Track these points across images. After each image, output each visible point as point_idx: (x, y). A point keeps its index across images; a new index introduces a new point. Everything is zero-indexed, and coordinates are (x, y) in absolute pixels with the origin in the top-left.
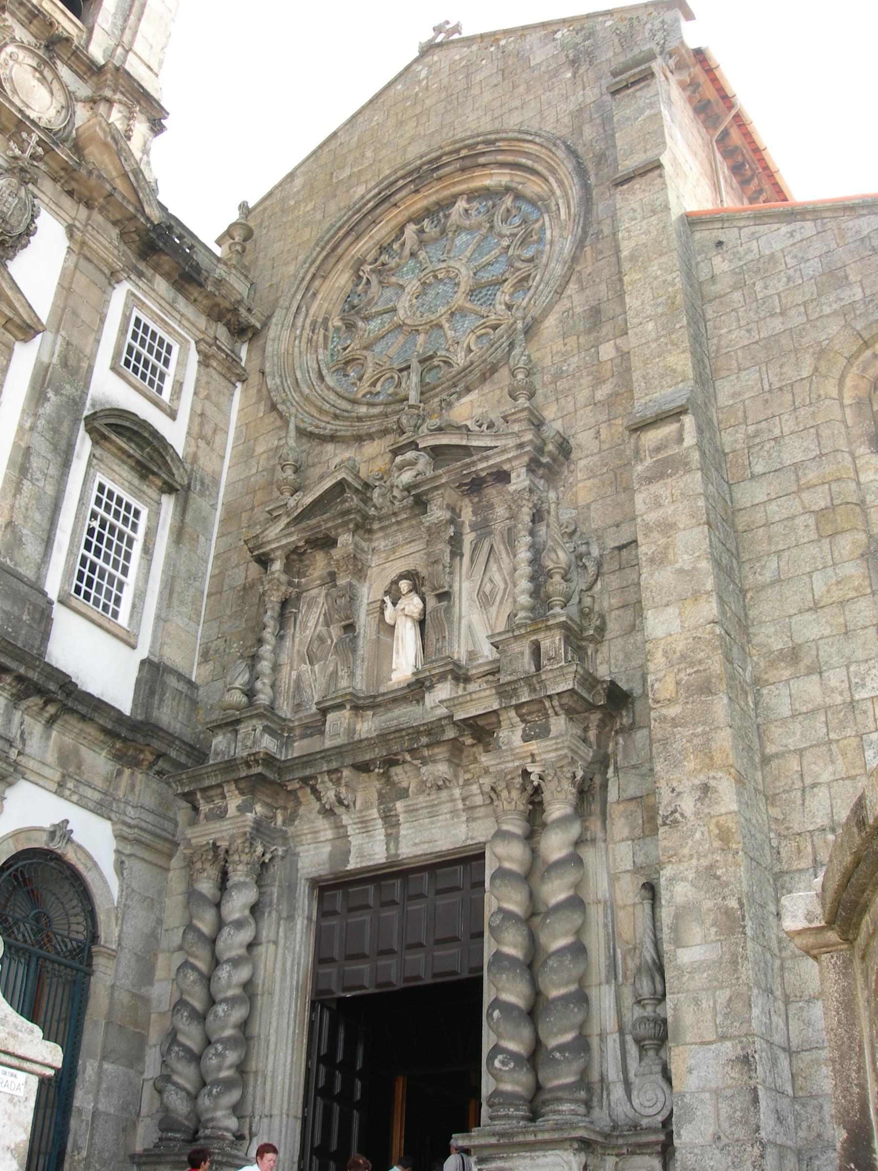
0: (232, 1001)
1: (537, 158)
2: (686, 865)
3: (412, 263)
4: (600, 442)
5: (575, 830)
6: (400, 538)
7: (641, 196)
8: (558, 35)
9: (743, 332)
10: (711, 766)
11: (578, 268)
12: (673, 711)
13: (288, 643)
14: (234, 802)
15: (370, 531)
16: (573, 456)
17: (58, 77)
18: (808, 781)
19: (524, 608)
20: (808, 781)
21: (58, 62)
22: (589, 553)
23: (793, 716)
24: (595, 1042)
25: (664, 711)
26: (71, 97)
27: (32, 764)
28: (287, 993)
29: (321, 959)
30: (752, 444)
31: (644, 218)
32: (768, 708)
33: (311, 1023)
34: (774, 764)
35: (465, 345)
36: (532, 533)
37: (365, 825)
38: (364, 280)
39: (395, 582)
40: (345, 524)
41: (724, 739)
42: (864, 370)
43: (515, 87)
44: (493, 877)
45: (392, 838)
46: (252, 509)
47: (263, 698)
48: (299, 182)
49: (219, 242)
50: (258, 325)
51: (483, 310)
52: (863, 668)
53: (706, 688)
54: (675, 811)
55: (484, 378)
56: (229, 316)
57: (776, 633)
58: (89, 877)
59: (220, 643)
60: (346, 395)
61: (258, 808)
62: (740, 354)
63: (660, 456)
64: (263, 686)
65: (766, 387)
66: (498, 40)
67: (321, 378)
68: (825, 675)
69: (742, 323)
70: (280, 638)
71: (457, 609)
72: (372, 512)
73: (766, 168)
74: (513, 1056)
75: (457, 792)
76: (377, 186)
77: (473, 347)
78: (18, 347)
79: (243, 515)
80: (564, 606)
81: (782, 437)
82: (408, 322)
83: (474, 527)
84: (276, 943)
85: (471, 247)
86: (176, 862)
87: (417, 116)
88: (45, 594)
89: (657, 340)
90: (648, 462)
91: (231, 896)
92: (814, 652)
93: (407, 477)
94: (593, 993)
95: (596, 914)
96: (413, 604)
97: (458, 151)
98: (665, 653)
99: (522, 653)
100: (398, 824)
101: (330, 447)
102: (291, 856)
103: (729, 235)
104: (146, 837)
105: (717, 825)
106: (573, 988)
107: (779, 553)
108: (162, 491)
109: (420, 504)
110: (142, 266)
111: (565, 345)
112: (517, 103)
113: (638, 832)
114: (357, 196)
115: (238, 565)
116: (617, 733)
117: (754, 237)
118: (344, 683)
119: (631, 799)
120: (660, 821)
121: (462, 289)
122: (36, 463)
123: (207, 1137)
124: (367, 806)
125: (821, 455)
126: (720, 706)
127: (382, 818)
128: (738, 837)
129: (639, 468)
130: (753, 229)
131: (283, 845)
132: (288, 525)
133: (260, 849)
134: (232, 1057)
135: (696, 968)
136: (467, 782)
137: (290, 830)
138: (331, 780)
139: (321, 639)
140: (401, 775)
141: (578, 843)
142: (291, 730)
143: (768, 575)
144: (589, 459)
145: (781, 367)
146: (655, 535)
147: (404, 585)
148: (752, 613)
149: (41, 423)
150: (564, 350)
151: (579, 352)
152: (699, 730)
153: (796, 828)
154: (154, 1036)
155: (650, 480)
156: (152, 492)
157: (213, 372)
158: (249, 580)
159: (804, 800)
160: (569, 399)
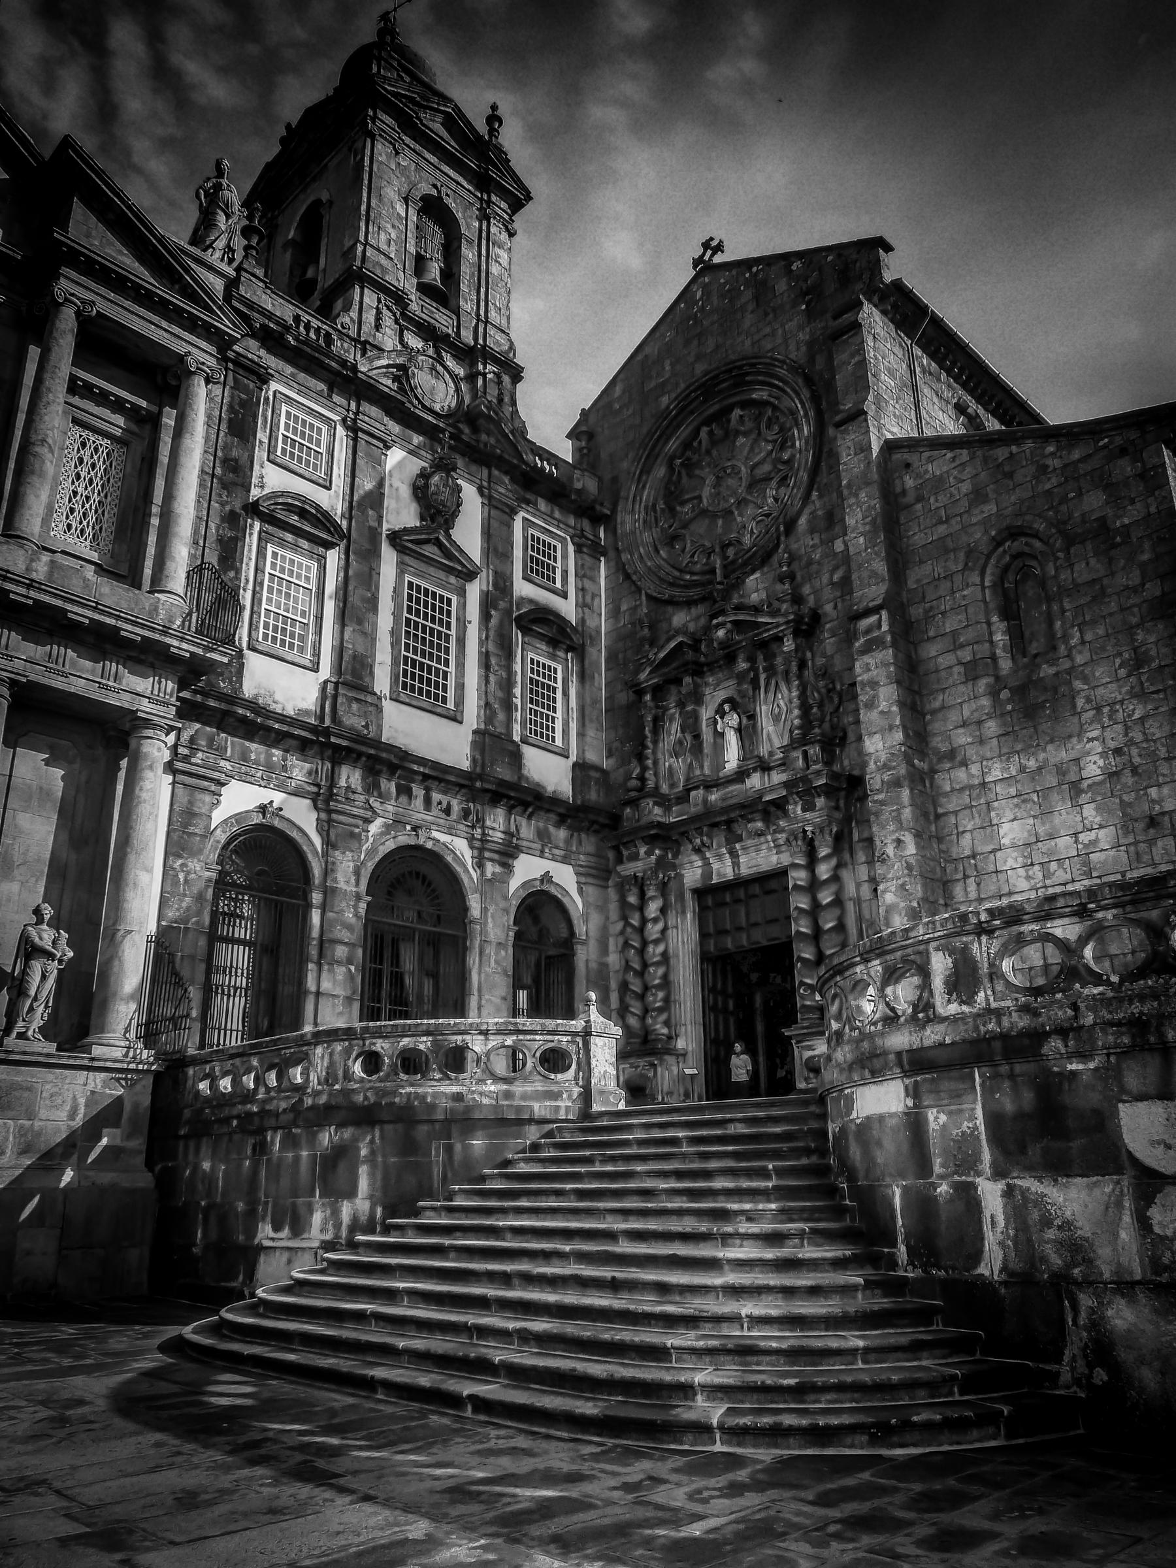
0: (657, 964)
1: (785, 382)
3: (707, 459)
5: (834, 862)
6: (720, 675)
8: (794, 267)
11: (818, 479)
12: (881, 797)
13: (661, 745)
16: (823, 620)
17: (446, 368)
18: (961, 829)
20: (961, 829)
21: (444, 354)
22: (834, 688)
23: (953, 790)
27: (525, 843)
29: (704, 935)
30: (929, 617)
31: (856, 454)
32: (938, 787)
34: (943, 819)
36: (800, 676)
37: (720, 857)
39: (721, 705)
40: (686, 671)
41: (907, 813)
42: (998, 562)
43: (766, 314)
45: (736, 864)
47: (651, 784)
48: (618, 390)
52: (990, 763)
53: (896, 783)
57: (942, 741)
58: (565, 900)
61: (657, 852)
64: (649, 774)
72: (702, 659)
75: (769, 838)
76: (676, 398)
78: (468, 587)
79: (620, 656)
80: (820, 727)
84: (677, 927)
85: (747, 449)
86: (610, 883)
88: (514, 742)
89: (866, 549)
90: (862, 640)
93: (721, 633)
95: (850, 907)
96: (733, 719)
97: (730, 371)
98: (875, 763)
100: (738, 856)
101: (670, 609)
102: (680, 877)
103: (913, 458)
104: (593, 872)
108: (567, 652)
109: (731, 659)
110: (529, 496)
112: (768, 330)
114: (663, 406)
117: (930, 460)
118: (698, 772)
121: (743, 484)
122: (493, 661)
123: (655, 1040)
124: (719, 847)
125: (967, 626)
126: (905, 794)
128: (916, 868)
132: (650, 673)
133: (661, 876)
134: (661, 995)
136: (775, 832)
137: (677, 862)
139: (680, 742)
140: (738, 829)
141: (839, 866)
142: (669, 800)
143: (937, 704)
146: (868, 689)
147: (727, 707)
148: (929, 728)
149: (492, 633)
150: (811, 543)
153: (955, 857)
154: (614, 985)
156: (561, 654)
157: (586, 557)
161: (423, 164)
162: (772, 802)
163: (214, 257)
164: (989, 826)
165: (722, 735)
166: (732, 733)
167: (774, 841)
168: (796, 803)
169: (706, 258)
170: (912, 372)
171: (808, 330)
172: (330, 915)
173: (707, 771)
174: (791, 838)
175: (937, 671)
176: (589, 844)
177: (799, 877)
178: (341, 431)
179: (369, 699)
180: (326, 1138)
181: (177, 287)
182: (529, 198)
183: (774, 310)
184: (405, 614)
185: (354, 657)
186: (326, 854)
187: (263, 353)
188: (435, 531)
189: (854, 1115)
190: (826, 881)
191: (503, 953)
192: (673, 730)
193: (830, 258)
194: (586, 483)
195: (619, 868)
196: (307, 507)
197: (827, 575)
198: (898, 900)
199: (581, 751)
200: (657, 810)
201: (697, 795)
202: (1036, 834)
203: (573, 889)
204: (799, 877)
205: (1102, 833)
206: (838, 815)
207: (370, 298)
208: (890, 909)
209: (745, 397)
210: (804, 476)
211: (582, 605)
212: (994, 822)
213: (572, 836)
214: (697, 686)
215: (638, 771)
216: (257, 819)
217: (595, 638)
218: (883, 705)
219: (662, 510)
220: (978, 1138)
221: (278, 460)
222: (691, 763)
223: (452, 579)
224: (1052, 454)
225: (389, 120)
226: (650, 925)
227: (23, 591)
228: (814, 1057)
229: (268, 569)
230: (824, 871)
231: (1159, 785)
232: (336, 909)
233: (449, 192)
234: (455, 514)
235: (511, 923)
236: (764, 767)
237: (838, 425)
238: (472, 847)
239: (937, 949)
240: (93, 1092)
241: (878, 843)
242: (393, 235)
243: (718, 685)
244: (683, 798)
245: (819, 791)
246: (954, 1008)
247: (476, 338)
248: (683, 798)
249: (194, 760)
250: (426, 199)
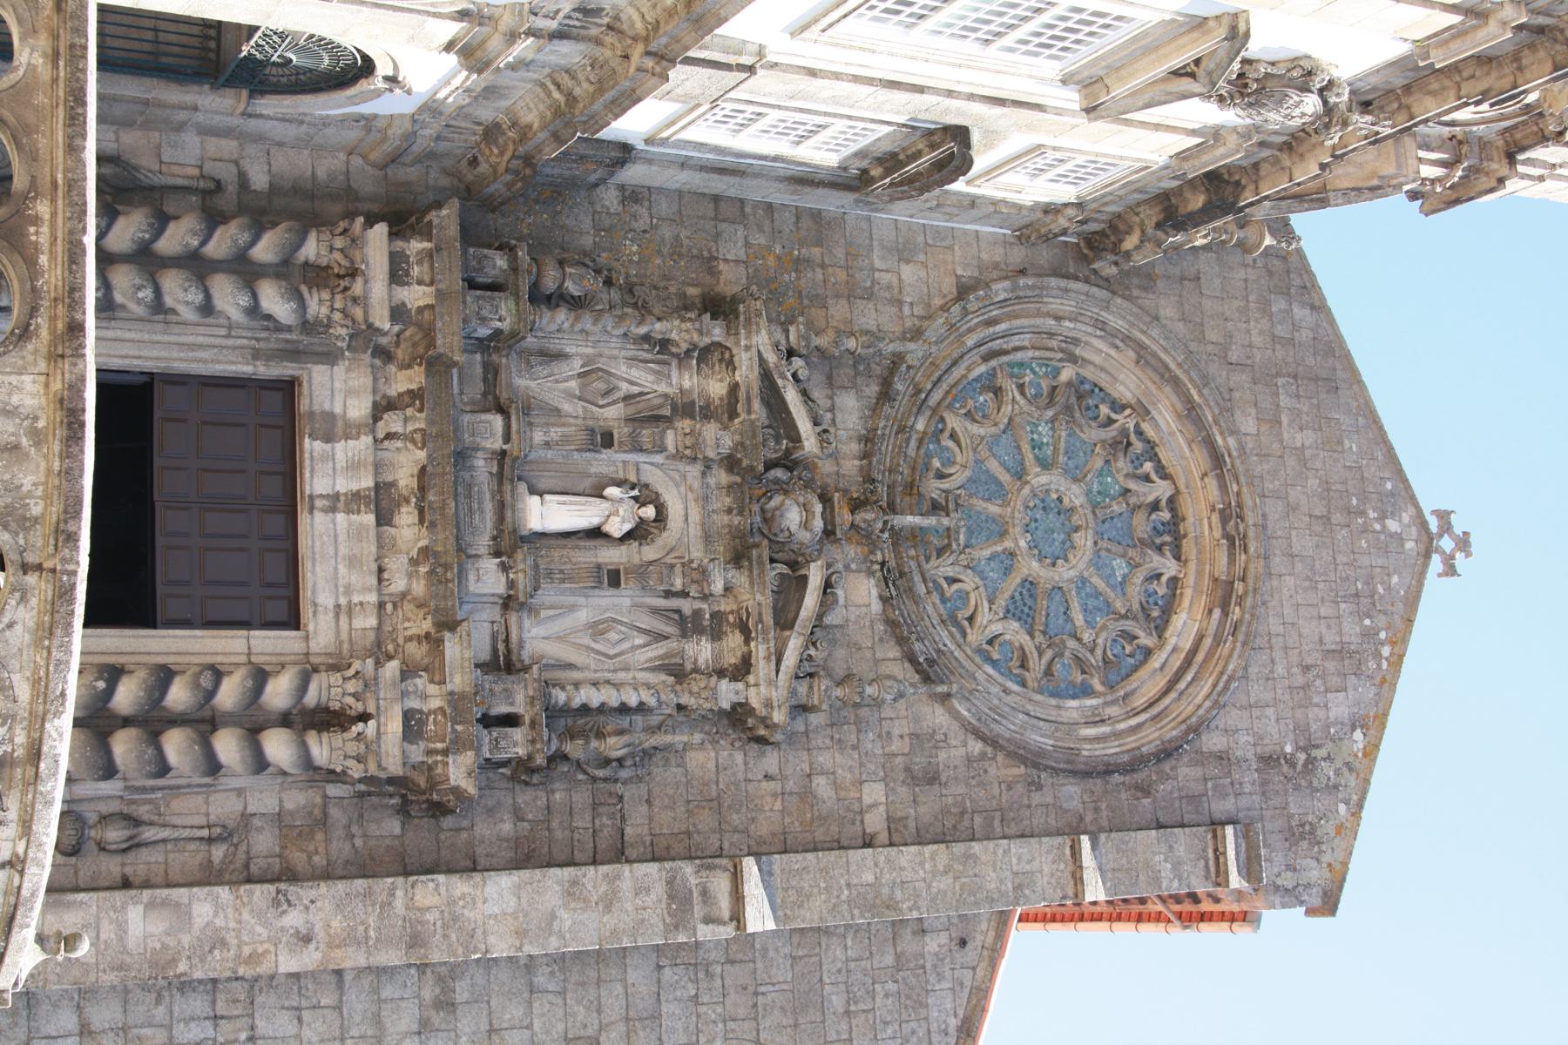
2: (231, 916)
4: (759, 781)
7: (1046, 870)
8: (1358, 735)
9: (839, 965)
10: (330, 946)
11: (1000, 757)
19: (569, 699)
20: (306, 1015)
23: (380, 1001)
25: (399, 893)
28: (164, 354)
35: (962, 577)
37: (353, 467)
38: (1114, 416)
45: (334, 502)
46: (823, 266)
50: (1095, 266)
53: (416, 940)
54: (288, 901)
55: (891, 624)
56: (1113, 239)
59: (643, 223)
62: (814, 959)
63: (695, 895)
65: (762, 989)
66: (1393, 644)
68: (416, 1039)
69: (852, 965)
73: (1119, 918)
77: (956, 586)
79: (816, 251)
81: (697, 1003)
82: (1026, 490)
83: (697, 614)
84: (228, 336)
87: (1326, 519)
90: (693, 881)
91: (289, 300)
92: (443, 1026)
97: (1243, 579)
98: (463, 897)
99: (512, 704)
100: (349, 511)
101: (873, 389)
105: (267, 952)
107: (562, 993)
111: (902, 737)
112: (1280, 670)
113: (287, 820)
115: (747, 244)
116: (403, 796)
119: (325, 814)
120: (283, 886)
127: (359, 491)
130: (968, 984)
131: (349, 346)
132: (762, 361)
135: (122, 929)
138: (415, 431)
144: (743, 767)
145: (782, 1008)
146: (604, 888)
147: (649, 512)
150: (896, 732)
151: (885, 755)
152: (372, 934)
153: (260, 1000)
155: (670, 882)
158: (722, 266)
159: (287, 1009)
160: (828, 741)
166: (595, 521)
167: (361, 604)
171: (1250, 755)
183: (1306, 687)
193: (1342, 808)
197: (829, 764)
198: (196, 931)
208: (183, 913)
213: (479, 124)
218: (566, 918)
236: (508, 603)
241: (313, 893)
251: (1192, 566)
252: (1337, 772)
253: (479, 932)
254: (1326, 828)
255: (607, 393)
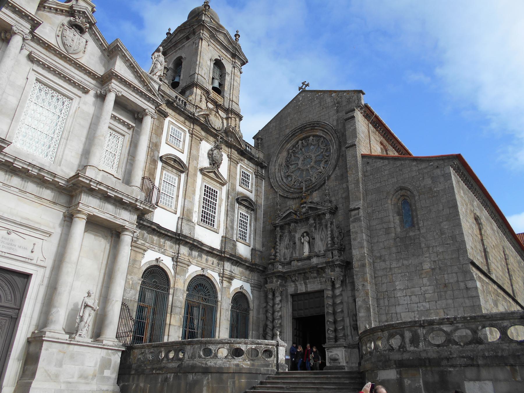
0: (278, 319)
5: (341, 289)
8: (333, 95)
13: (282, 245)
14: (275, 280)
15: (298, 222)
16: (338, 209)
17: (219, 115)
19: (329, 244)
20: (383, 282)
21: (219, 110)
24: (346, 328)
25: (356, 270)
26: (222, 119)
29: (293, 310)
33: (293, 322)
36: (330, 227)
37: (301, 284)
39: (303, 233)
43: (323, 109)
44: (326, 298)
45: (306, 287)
49: (253, 138)
51: (318, 167)
55: (319, 188)
58: (247, 295)
60: (289, 185)
61: (280, 281)
67: (283, 180)
70: (280, 243)
71: (316, 242)
74: (332, 331)
75: (318, 279)
82: (301, 168)
83: (319, 224)
85: (314, 150)
87: (300, 112)
88: (234, 241)
90: (353, 218)
93: (304, 210)
94: (345, 319)
95: (345, 304)
96: (307, 238)
97: (310, 124)
101: (286, 199)
102: (287, 290)
103: (370, 161)
106: (341, 318)
108: (251, 211)
110: (242, 158)
112: (323, 114)
114: (287, 133)
117: (375, 162)
119: (351, 283)
122: (229, 212)
129: (351, 219)
136: (320, 277)
139: (289, 245)
142: (284, 264)
143: (376, 241)
147: (305, 234)
149: (229, 204)
156: (250, 212)
161: (216, 48)
162: (321, 268)
163: (156, 78)
164: (392, 282)
165: (303, 243)
168: (328, 269)
169: (303, 87)
170: (369, 132)
172: (175, 297)
173: (297, 255)
174: (327, 280)
175: (376, 230)
176: (255, 276)
177: (329, 293)
178: (188, 135)
179: (192, 224)
180: (191, 377)
181: (145, 87)
182: (247, 62)
184: (203, 196)
185: (188, 210)
186: (175, 277)
187: (166, 108)
188: (214, 169)
189: (378, 379)
190: (339, 296)
191: (227, 313)
192: (286, 240)
193: (345, 94)
194: (259, 155)
195: (266, 286)
196: (176, 159)
199: (254, 245)
200: (280, 267)
201: (294, 263)
202: (408, 286)
203: (249, 290)
204: (329, 293)
205: (429, 288)
206: (342, 274)
207: (199, 91)
208: (360, 307)
209: (314, 133)
210: (333, 161)
211: (257, 195)
212: (394, 281)
214: (295, 227)
215: (274, 253)
216: (154, 263)
217: (260, 207)
219: (285, 166)
220: (421, 389)
221: (169, 143)
222: (292, 252)
223: (218, 185)
224: (415, 165)
225: (207, 34)
226: (276, 306)
227: (95, 185)
228: (333, 355)
229: (163, 179)
230: (338, 292)
231: (448, 274)
232: (177, 296)
233: (224, 58)
234: (221, 163)
235: (230, 302)
236: (318, 256)
237: (347, 148)
238: (219, 276)
239: (407, 330)
240: (103, 357)
241: (356, 284)
242: (206, 72)
243: (302, 227)
244: (289, 263)
245: (337, 266)
246: (412, 348)
247: (229, 106)
248: (289, 263)
249: (137, 242)
250: (216, 60)
251: (310, 134)
252: (339, 97)
253: (362, 255)
254: (348, 96)
255: (289, 245)
